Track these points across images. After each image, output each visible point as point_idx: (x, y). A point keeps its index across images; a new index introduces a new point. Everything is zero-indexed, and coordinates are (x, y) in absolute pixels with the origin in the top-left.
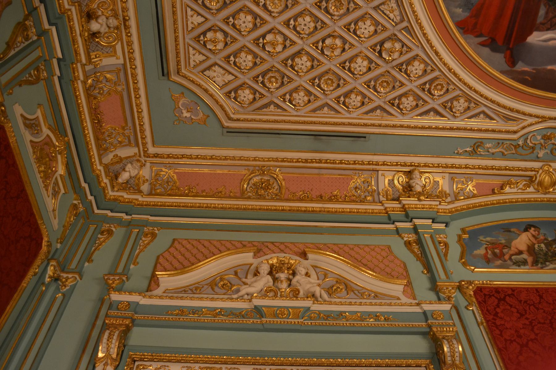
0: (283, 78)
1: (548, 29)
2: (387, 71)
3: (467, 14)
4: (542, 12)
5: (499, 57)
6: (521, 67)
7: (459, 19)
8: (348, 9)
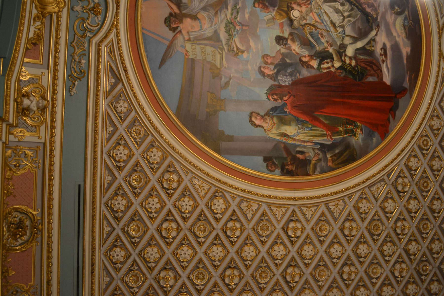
0: (423, 261)
1: (381, 71)
2: (416, 185)
3: (376, 134)
4: (371, 79)
5: (402, 102)
6: (406, 84)
7: (380, 138)
8: (378, 220)
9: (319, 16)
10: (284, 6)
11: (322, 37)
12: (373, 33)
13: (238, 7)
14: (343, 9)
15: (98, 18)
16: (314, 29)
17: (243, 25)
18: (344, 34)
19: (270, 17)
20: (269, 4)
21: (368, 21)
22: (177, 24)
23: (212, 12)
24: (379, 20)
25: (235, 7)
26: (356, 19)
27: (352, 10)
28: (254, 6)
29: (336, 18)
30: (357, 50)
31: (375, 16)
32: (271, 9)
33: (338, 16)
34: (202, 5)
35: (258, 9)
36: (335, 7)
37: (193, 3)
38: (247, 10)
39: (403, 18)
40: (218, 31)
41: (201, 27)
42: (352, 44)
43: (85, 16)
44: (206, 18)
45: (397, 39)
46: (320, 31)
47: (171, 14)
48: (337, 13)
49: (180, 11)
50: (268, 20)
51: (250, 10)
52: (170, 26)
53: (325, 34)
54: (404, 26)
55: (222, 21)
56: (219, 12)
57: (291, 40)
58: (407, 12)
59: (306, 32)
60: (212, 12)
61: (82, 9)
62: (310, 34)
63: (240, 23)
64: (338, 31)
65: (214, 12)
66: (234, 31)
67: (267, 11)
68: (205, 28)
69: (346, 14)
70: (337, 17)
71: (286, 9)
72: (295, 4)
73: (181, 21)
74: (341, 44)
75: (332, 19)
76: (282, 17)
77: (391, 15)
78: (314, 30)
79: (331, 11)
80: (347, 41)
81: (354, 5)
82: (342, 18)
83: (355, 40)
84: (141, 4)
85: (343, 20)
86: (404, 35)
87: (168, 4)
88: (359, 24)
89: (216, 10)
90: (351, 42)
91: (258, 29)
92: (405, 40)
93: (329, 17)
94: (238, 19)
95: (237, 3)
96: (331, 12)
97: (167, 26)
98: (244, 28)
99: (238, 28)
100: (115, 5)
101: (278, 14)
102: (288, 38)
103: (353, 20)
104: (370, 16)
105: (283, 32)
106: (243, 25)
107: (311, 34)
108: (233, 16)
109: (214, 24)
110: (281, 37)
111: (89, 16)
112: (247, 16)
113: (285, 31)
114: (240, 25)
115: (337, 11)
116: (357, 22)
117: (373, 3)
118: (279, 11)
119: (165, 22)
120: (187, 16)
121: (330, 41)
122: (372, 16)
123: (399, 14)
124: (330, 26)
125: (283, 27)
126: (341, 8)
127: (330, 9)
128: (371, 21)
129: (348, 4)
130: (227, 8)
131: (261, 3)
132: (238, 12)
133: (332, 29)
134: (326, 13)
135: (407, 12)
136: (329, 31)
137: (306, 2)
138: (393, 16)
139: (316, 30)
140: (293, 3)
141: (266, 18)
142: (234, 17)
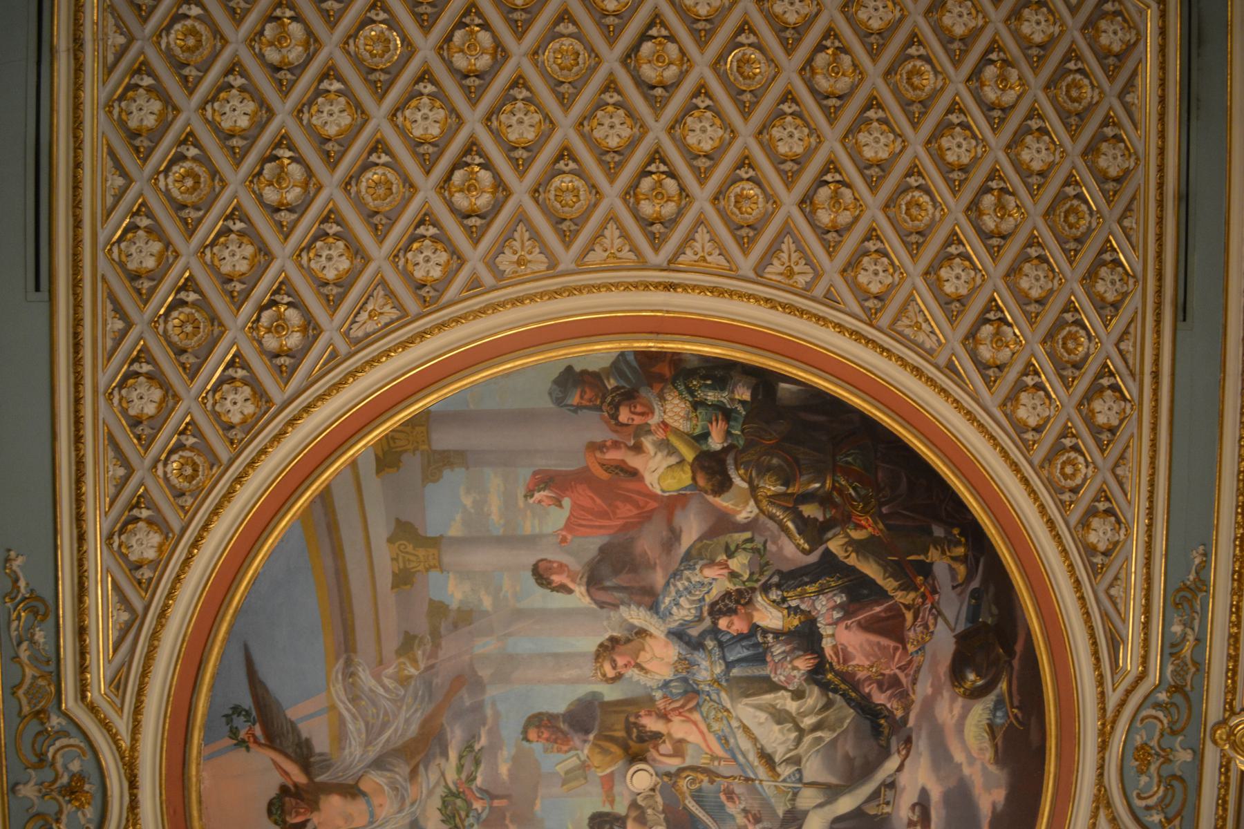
9: (724, 740)
10: (616, 727)
11: (730, 799)
12: (892, 764)
13: (477, 747)
14: (800, 707)
15: (84, 815)
16: (706, 779)
17: (493, 797)
18: (800, 780)
19: (572, 762)
20: (572, 726)
21: (876, 731)
22: (304, 814)
23: (404, 770)
24: (911, 723)
25: (470, 747)
26: (839, 731)
27: (828, 705)
28: (526, 739)
29: (776, 739)
30: (838, 820)
31: (899, 714)
32: (576, 740)
33: (781, 731)
34: (373, 753)
35: (537, 747)
36: (774, 707)
37: (347, 751)
38: (506, 753)
39: (991, 705)
40: (422, 822)
41: (372, 815)
42: (820, 806)
43: (50, 807)
44: (386, 788)
45: (966, 771)
46: (723, 784)
47: (284, 790)
48: (779, 722)
49: (311, 779)
50: (567, 773)
51: (513, 751)
52: (284, 822)
53: (739, 789)
54: (992, 728)
55: (430, 793)
56: (421, 768)
57: (635, 819)
58: (1003, 685)
59: (682, 793)
60: (403, 769)
61: (40, 791)
62: (693, 797)
63: (486, 791)
64: (779, 775)
65: (407, 770)
66: (467, 816)
67: (565, 748)
68: (383, 815)
69: (808, 722)
70: (780, 736)
71: (621, 734)
72: (649, 714)
73: (314, 806)
74: (787, 812)
75: (764, 742)
76: (608, 758)
77: (953, 700)
78: (706, 783)
79: (762, 720)
80: (808, 798)
81: (835, 691)
82: (794, 735)
83: (832, 792)
84: (198, 771)
85: (799, 741)
86: (989, 754)
87: (275, 763)
88: (849, 747)
89: (413, 763)
90: (819, 801)
91: (538, 802)
92: (993, 769)
93: (755, 740)
94: (479, 781)
95: (474, 737)
96: (761, 724)
97: (276, 823)
98: (496, 803)
99: (477, 805)
100: (126, 785)
101: (598, 750)
102: (626, 817)
103: (827, 736)
104: (885, 717)
105: (612, 802)
106: (493, 797)
107: (698, 797)
108: (464, 776)
109: (408, 802)
110: (608, 814)
111: (60, 812)
112: (504, 769)
113: (618, 799)
114: (485, 796)
115: (780, 717)
116: (839, 743)
117: (895, 675)
118: (602, 743)
119: (270, 813)
120: (329, 789)
121: (755, 806)
122: (890, 716)
123: (976, 694)
124: (756, 764)
125: (611, 788)
126: (792, 706)
127: (759, 713)
128: (886, 731)
129: (816, 690)
130: (445, 754)
131: (547, 727)
132: (477, 763)
133: (762, 772)
134: (746, 729)
135: (1003, 685)
136: (753, 780)
137: (682, 706)
138: (960, 701)
139: (712, 782)
140: (642, 713)
141: (561, 769)
142: (468, 777)
